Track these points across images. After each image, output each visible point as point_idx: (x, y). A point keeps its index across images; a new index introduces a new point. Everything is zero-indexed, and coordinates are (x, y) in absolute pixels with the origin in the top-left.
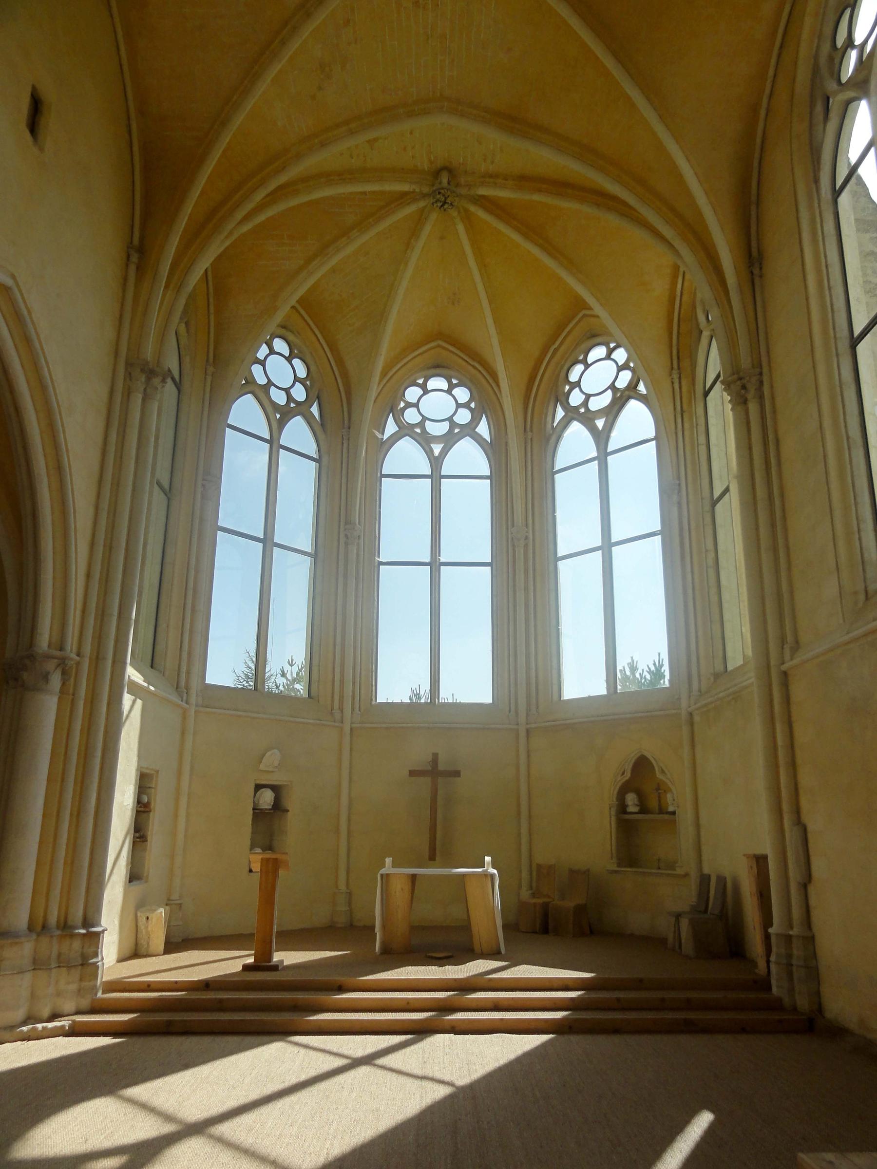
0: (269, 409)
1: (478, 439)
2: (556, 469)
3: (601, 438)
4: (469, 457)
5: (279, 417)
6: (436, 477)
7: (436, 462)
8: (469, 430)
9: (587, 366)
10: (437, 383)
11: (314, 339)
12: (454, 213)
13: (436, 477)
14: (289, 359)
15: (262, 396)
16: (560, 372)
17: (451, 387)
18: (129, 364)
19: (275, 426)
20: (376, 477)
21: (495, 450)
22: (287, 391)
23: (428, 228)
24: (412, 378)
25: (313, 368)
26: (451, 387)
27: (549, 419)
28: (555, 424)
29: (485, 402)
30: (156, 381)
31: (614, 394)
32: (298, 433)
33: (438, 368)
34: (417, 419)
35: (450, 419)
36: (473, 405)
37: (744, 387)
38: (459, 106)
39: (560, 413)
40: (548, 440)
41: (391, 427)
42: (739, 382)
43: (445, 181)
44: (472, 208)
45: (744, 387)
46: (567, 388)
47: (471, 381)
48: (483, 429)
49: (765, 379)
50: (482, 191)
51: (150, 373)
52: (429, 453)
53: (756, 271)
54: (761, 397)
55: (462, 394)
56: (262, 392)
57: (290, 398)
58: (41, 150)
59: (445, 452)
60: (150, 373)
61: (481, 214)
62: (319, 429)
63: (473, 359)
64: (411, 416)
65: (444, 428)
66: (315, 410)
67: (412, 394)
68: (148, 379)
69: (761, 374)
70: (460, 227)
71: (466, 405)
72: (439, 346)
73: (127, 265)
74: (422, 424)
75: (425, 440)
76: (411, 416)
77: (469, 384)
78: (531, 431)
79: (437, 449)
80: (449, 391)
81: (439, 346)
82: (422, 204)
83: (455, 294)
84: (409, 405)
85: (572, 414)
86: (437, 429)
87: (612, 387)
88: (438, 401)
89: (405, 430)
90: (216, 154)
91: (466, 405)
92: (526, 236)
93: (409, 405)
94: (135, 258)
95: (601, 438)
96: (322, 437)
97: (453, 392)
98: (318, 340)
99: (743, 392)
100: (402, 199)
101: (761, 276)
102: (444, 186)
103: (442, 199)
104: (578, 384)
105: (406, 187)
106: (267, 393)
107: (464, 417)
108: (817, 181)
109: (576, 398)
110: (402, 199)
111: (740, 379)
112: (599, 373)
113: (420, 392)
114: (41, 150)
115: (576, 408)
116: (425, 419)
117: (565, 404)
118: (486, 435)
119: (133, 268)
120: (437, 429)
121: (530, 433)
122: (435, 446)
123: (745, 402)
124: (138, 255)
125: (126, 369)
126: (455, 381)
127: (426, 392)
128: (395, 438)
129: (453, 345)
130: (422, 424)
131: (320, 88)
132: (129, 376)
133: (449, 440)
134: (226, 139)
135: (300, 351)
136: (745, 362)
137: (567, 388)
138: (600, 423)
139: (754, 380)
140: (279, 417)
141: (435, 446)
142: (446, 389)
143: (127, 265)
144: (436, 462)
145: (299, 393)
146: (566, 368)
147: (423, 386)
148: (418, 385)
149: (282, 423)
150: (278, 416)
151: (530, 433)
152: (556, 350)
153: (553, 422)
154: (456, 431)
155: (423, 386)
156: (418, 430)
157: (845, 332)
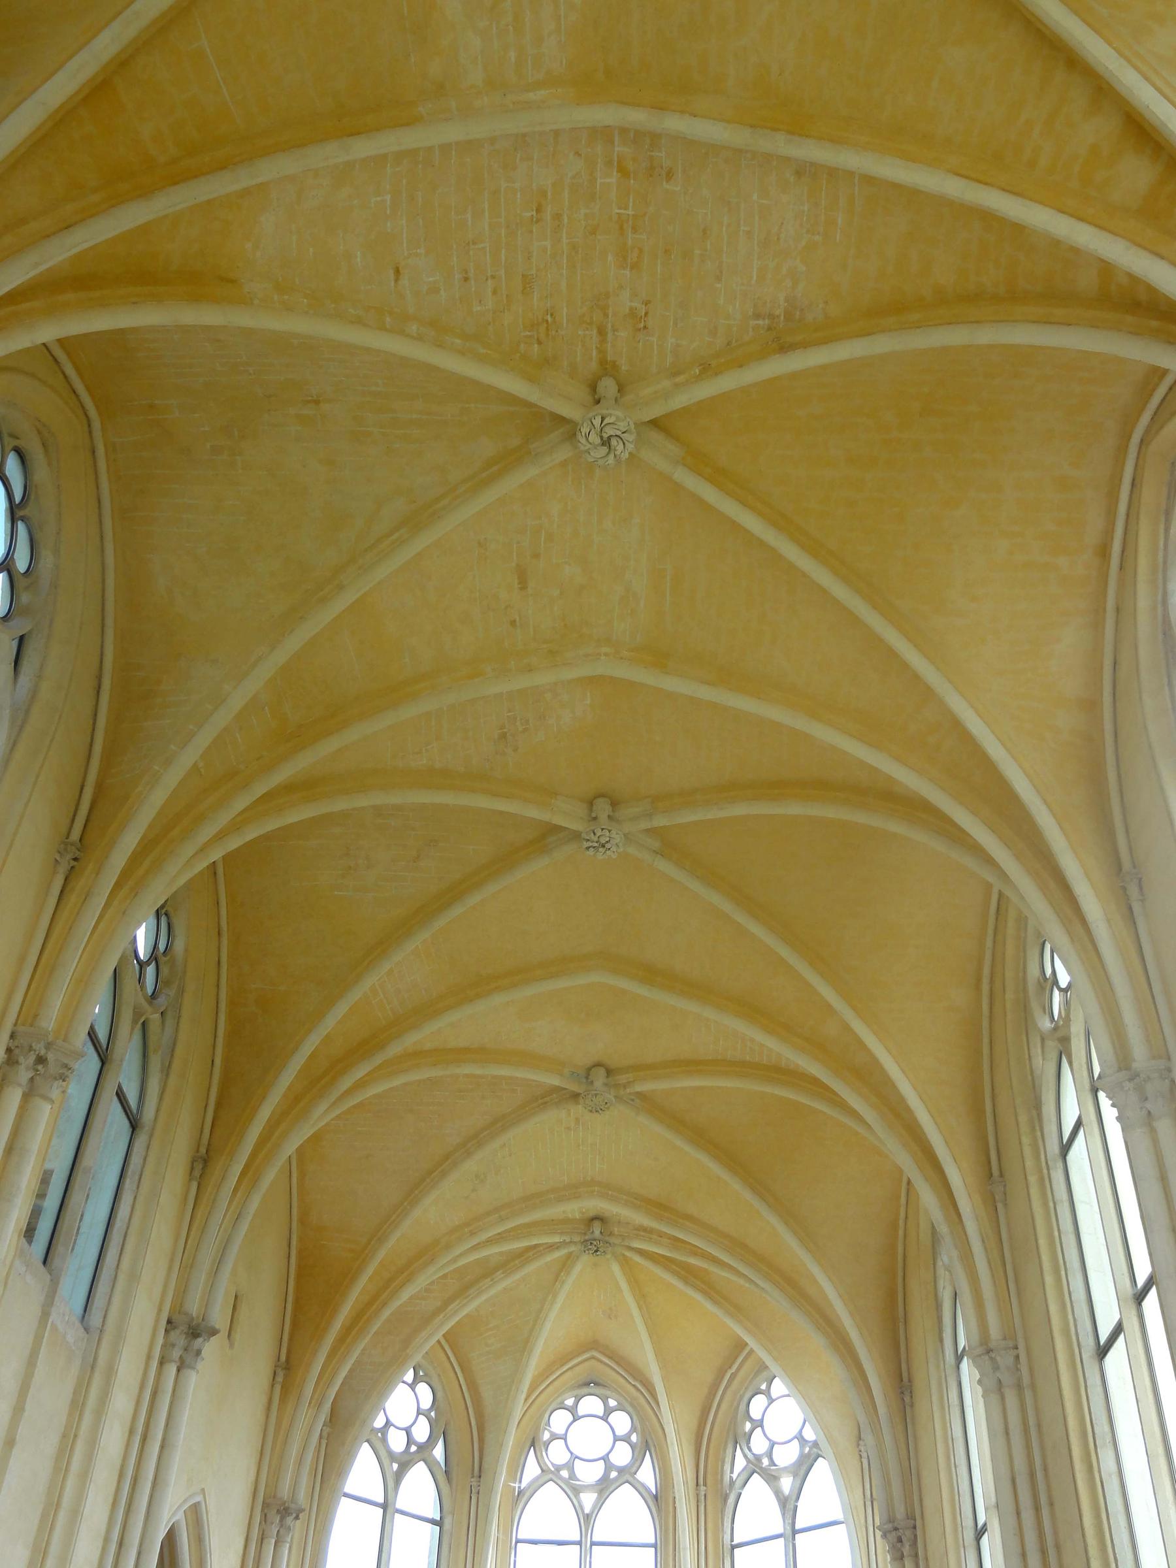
0: (386, 1462)
1: (640, 1488)
2: (735, 1542)
3: (788, 1505)
5: (396, 1469)
6: (586, 1544)
7: (587, 1520)
8: (627, 1474)
9: (771, 1401)
10: (591, 1404)
11: (444, 1358)
12: (609, 1256)
13: (586, 1544)
14: (412, 1386)
15: (379, 1445)
16: (739, 1405)
17: (608, 1411)
18: (266, 1505)
19: (391, 1484)
20: (510, 1544)
21: (660, 1502)
22: (408, 1431)
23: (578, 1268)
24: (559, 1399)
25: (439, 1394)
26: (608, 1411)
27: (727, 1467)
28: (734, 1476)
29: (648, 1441)
30: (289, 1520)
31: (802, 1447)
32: (420, 1490)
33: (591, 1384)
35: (605, 1458)
37: (900, 1540)
38: (608, 1190)
39: (740, 1463)
40: (725, 1498)
41: (531, 1470)
42: (894, 1533)
43: (597, 1233)
44: (628, 1254)
45: (900, 1540)
46: (748, 1426)
47: (632, 1405)
48: (647, 1474)
49: (919, 1533)
50: (637, 1244)
51: (285, 1511)
52: (578, 1508)
53: (907, 1399)
54: (916, 1555)
55: (622, 1422)
56: (379, 1440)
57: (410, 1440)
58: (231, 1346)
60: (285, 1511)
61: (637, 1259)
62: (446, 1476)
63: (635, 1378)
65: (598, 1470)
66: (438, 1452)
67: (559, 1420)
68: (281, 1520)
69: (915, 1527)
70: (616, 1268)
71: (626, 1439)
72: (593, 1358)
73: (273, 1386)
74: (570, 1466)
75: (573, 1490)
76: (557, 1454)
77: (630, 1409)
78: (705, 1484)
80: (605, 1418)
81: (593, 1358)
82: (572, 1248)
83: (611, 1309)
85: (755, 1466)
86: (589, 1473)
87: (800, 1437)
88: (589, 1432)
89: (549, 1474)
90: (370, 1270)
91: (626, 1439)
92: (686, 1282)
93: (555, 1437)
94: (280, 1379)
95: (788, 1505)
96: (445, 1489)
97: (611, 1418)
98: (448, 1358)
99: (899, 1545)
100: (552, 1247)
101: (912, 1406)
102: (595, 1234)
103: (594, 1246)
104: (759, 1424)
105: (557, 1239)
106: (384, 1440)
107: (622, 1455)
108: (941, 1340)
109: (758, 1444)
110: (552, 1247)
111: (896, 1529)
112: (781, 1417)
114: (231, 1346)
115: (758, 1458)
117: (746, 1451)
119: (278, 1388)
121: (703, 1488)
123: (902, 1557)
124: (286, 1370)
125: (262, 1510)
128: (536, 1485)
129: (610, 1358)
130: (570, 1466)
131: (474, 1190)
132: (265, 1517)
133: (604, 1487)
134: (381, 1254)
135: (426, 1375)
136: (900, 1512)
137: (748, 1426)
138: (786, 1484)
139: (908, 1533)
140: (396, 1469)
143: (273, 1386)
144: (587, 1520)
145: (422, 1432)
146: (745, 1399)
147: (573, 1410)
149: (399, 1476)
150: (395, 1466)
151: (703, 1488)
152: (733, 1376)
153: (732, 1472)
155: (573, 1410)
157: (969, 1522)
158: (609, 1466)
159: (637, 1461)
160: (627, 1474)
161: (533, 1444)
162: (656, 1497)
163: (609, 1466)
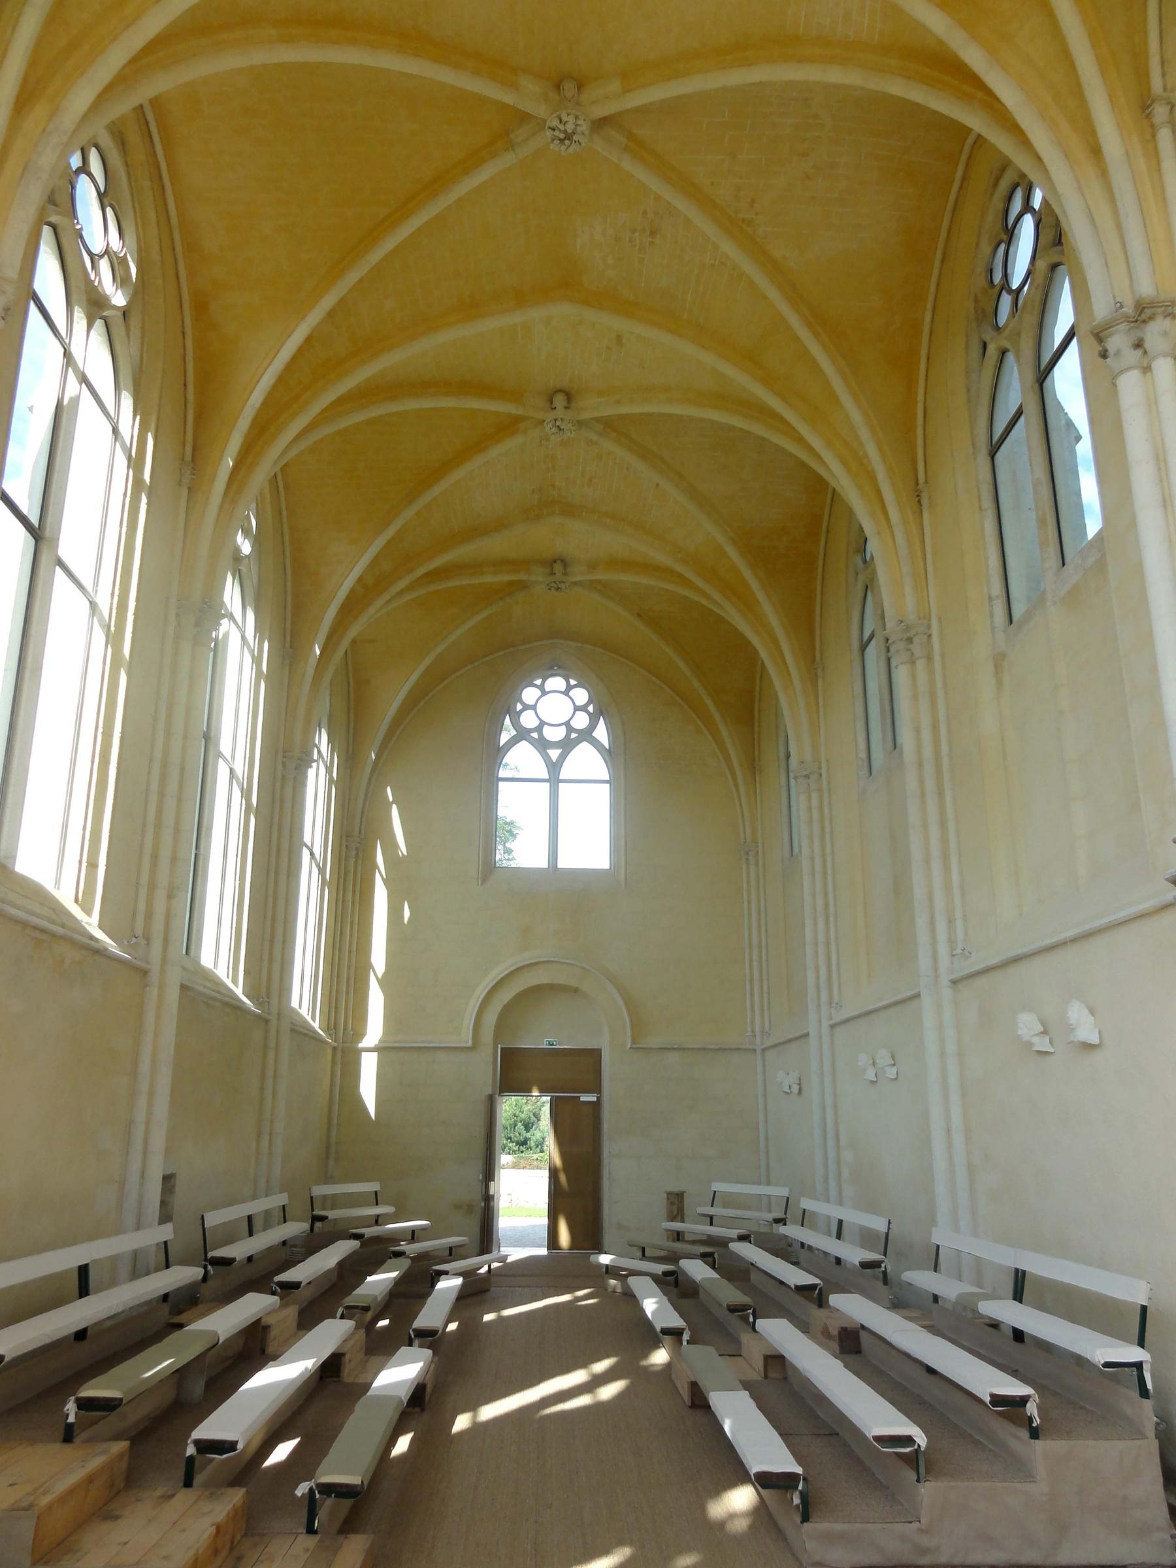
1: (595, 743)
4: (588, 762)
7: (554, 767)
8: (586, 735)
10: (556, 683)
17: (569, 688)
26: (569, 688)
29: (600, 709)
34: (536, 723)
35: (567, 724)
36: (591, 708)
48: (601, 733)
52: (547, 758)
55: (581, 695)
59: (563, 758)
64: (528, 720)
67: (529, 695)
71: (583, 708)
75: (542, 745)
76: (528, 720)
79: (554, 754)
80: (566, 693)
84: (526, 707)
86: (554, 734)
89: (522, 734)
91: (583, 708)
93: (526, 707)
107: (581, 721)
113: (538, 693)
116: (542, 723)
118: (605, 741)
120: (554, 734)
122: (555, 752)
126: (573, 682)
127: (544, 693)
133: (567, 745)
141: (555, 752)
142: (563, 689)
144: (554, 767)
147: (541, 688)
148: (536, 686)
154: (573, 735)
155: (541, 688)
156: (535, 735)
158: (570, 729)
159: (593, 726)
160: (586, 735)
161: (508, 712)
162: (609, 751)
163: (570, 729)
